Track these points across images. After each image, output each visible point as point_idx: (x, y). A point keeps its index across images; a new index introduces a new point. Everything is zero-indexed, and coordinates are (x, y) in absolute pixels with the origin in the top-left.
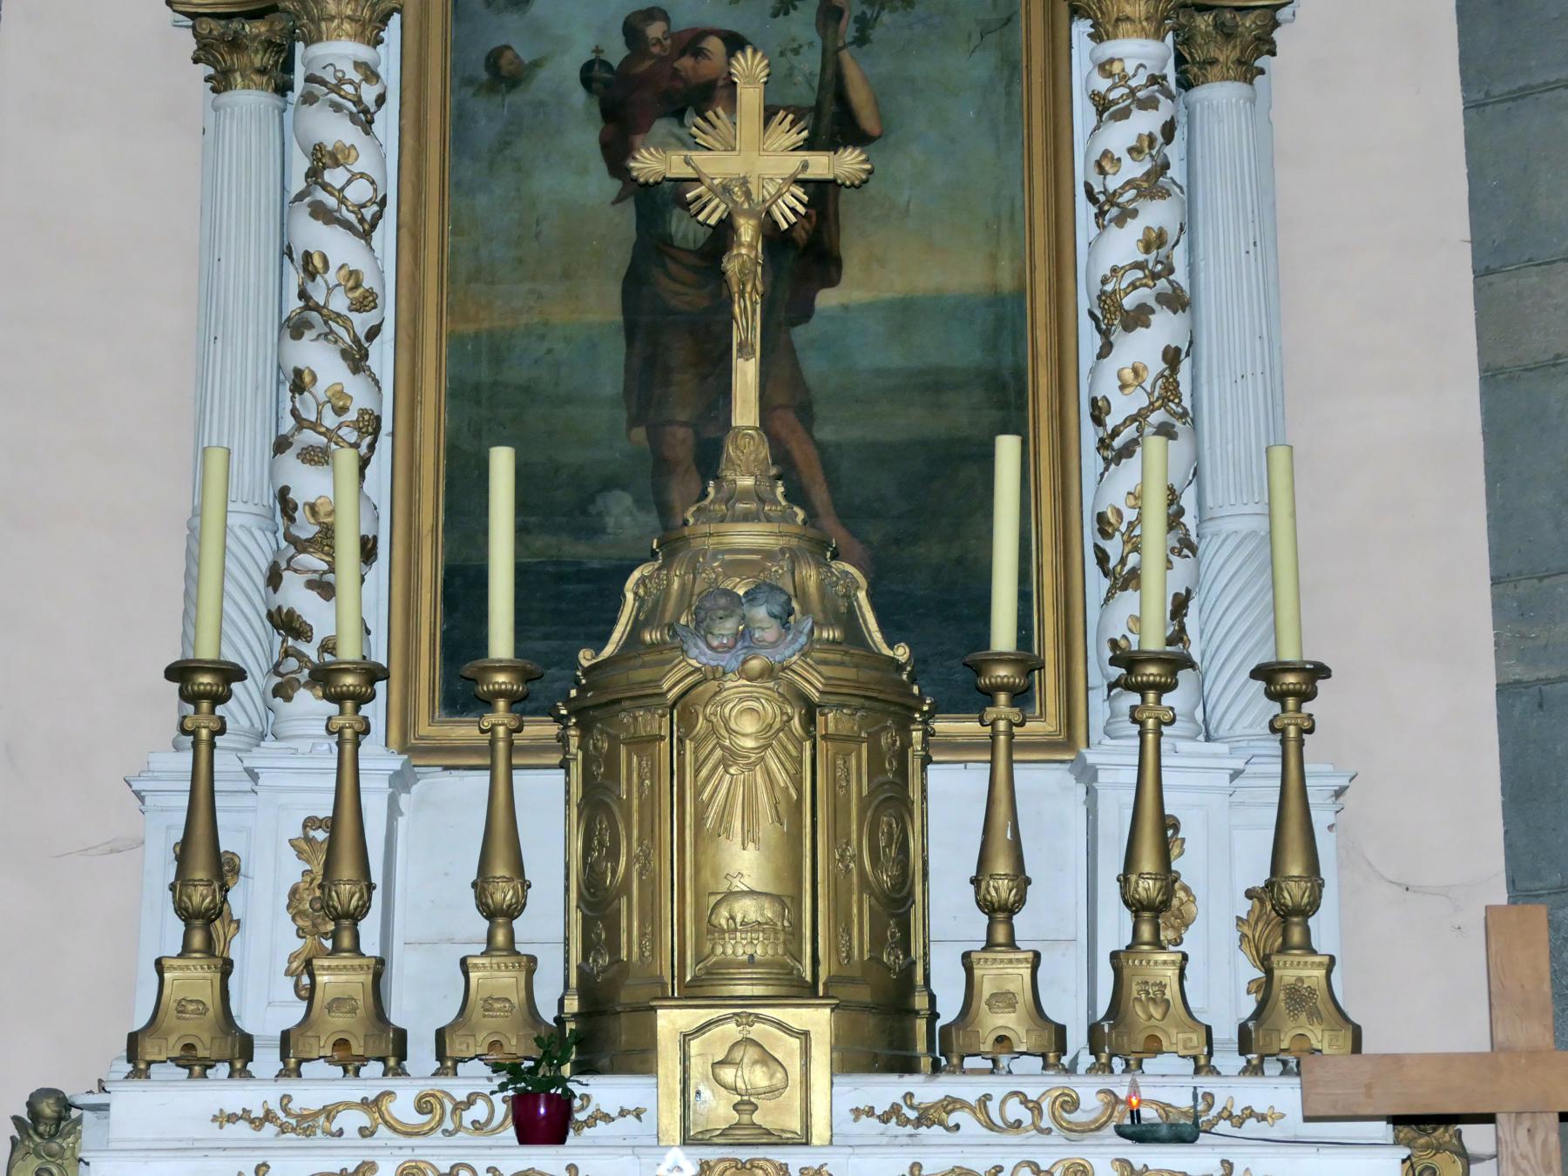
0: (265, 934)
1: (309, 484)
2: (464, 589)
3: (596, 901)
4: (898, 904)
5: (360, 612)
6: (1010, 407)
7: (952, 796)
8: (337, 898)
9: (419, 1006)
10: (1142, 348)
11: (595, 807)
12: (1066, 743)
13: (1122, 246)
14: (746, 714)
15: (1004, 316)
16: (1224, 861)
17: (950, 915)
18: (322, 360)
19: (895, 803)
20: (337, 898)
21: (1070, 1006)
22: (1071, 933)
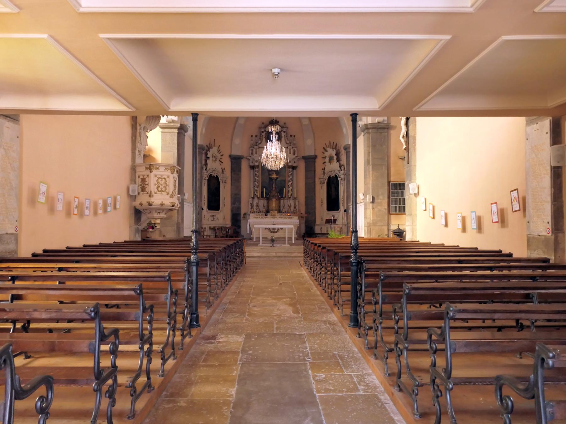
0: (255, 207)
1: (256, 188)
2: (262, 192)
3: (268, 207)
4: (280, 207)
5: (258, 194)
6: (285, 187)
7: (282, 201)
8: (258, 206)
9: (261, 210)
10: (290, 183)
11: (268, 203)
12: (287, 199)
13: (289, 179)
14: (274, 200)
15: (285, 181)
16: (292, 205)
17: (282, 208)
18: (256, 183)
19: (280, 203)
20: (258, 206)
21: (286, 210)
22: (287, 207)
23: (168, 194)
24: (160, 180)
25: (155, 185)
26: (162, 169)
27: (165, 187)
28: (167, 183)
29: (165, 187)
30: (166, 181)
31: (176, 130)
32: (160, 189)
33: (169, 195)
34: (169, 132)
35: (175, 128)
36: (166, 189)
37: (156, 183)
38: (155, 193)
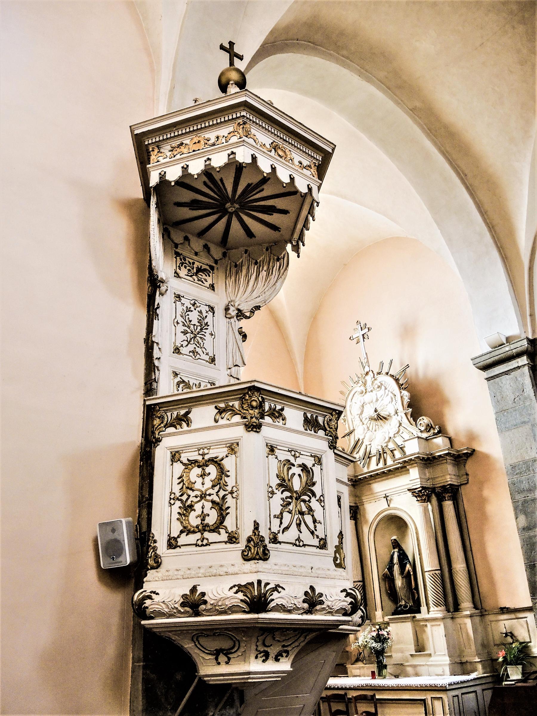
23: (232, 539)
24: (196, 471)
25: (173, 499)
26: (202, 415)
27: (220, 507)
28: (230, 482)
29: (220, 507)
30: (222, 472)
31: (524, 360)
32: (194, 520)
33: (242, 545)
34: (507, 373)
35: (519, 355)
36: (222, 518)
37: (177, 490)
38: (172, 543)
